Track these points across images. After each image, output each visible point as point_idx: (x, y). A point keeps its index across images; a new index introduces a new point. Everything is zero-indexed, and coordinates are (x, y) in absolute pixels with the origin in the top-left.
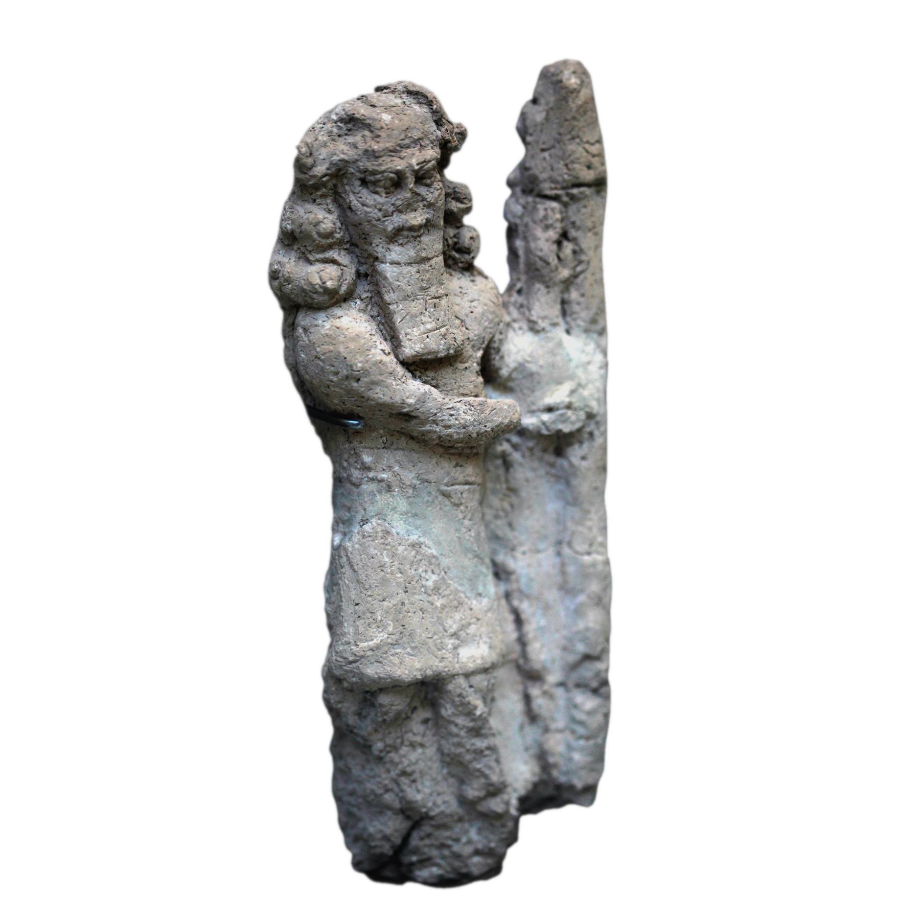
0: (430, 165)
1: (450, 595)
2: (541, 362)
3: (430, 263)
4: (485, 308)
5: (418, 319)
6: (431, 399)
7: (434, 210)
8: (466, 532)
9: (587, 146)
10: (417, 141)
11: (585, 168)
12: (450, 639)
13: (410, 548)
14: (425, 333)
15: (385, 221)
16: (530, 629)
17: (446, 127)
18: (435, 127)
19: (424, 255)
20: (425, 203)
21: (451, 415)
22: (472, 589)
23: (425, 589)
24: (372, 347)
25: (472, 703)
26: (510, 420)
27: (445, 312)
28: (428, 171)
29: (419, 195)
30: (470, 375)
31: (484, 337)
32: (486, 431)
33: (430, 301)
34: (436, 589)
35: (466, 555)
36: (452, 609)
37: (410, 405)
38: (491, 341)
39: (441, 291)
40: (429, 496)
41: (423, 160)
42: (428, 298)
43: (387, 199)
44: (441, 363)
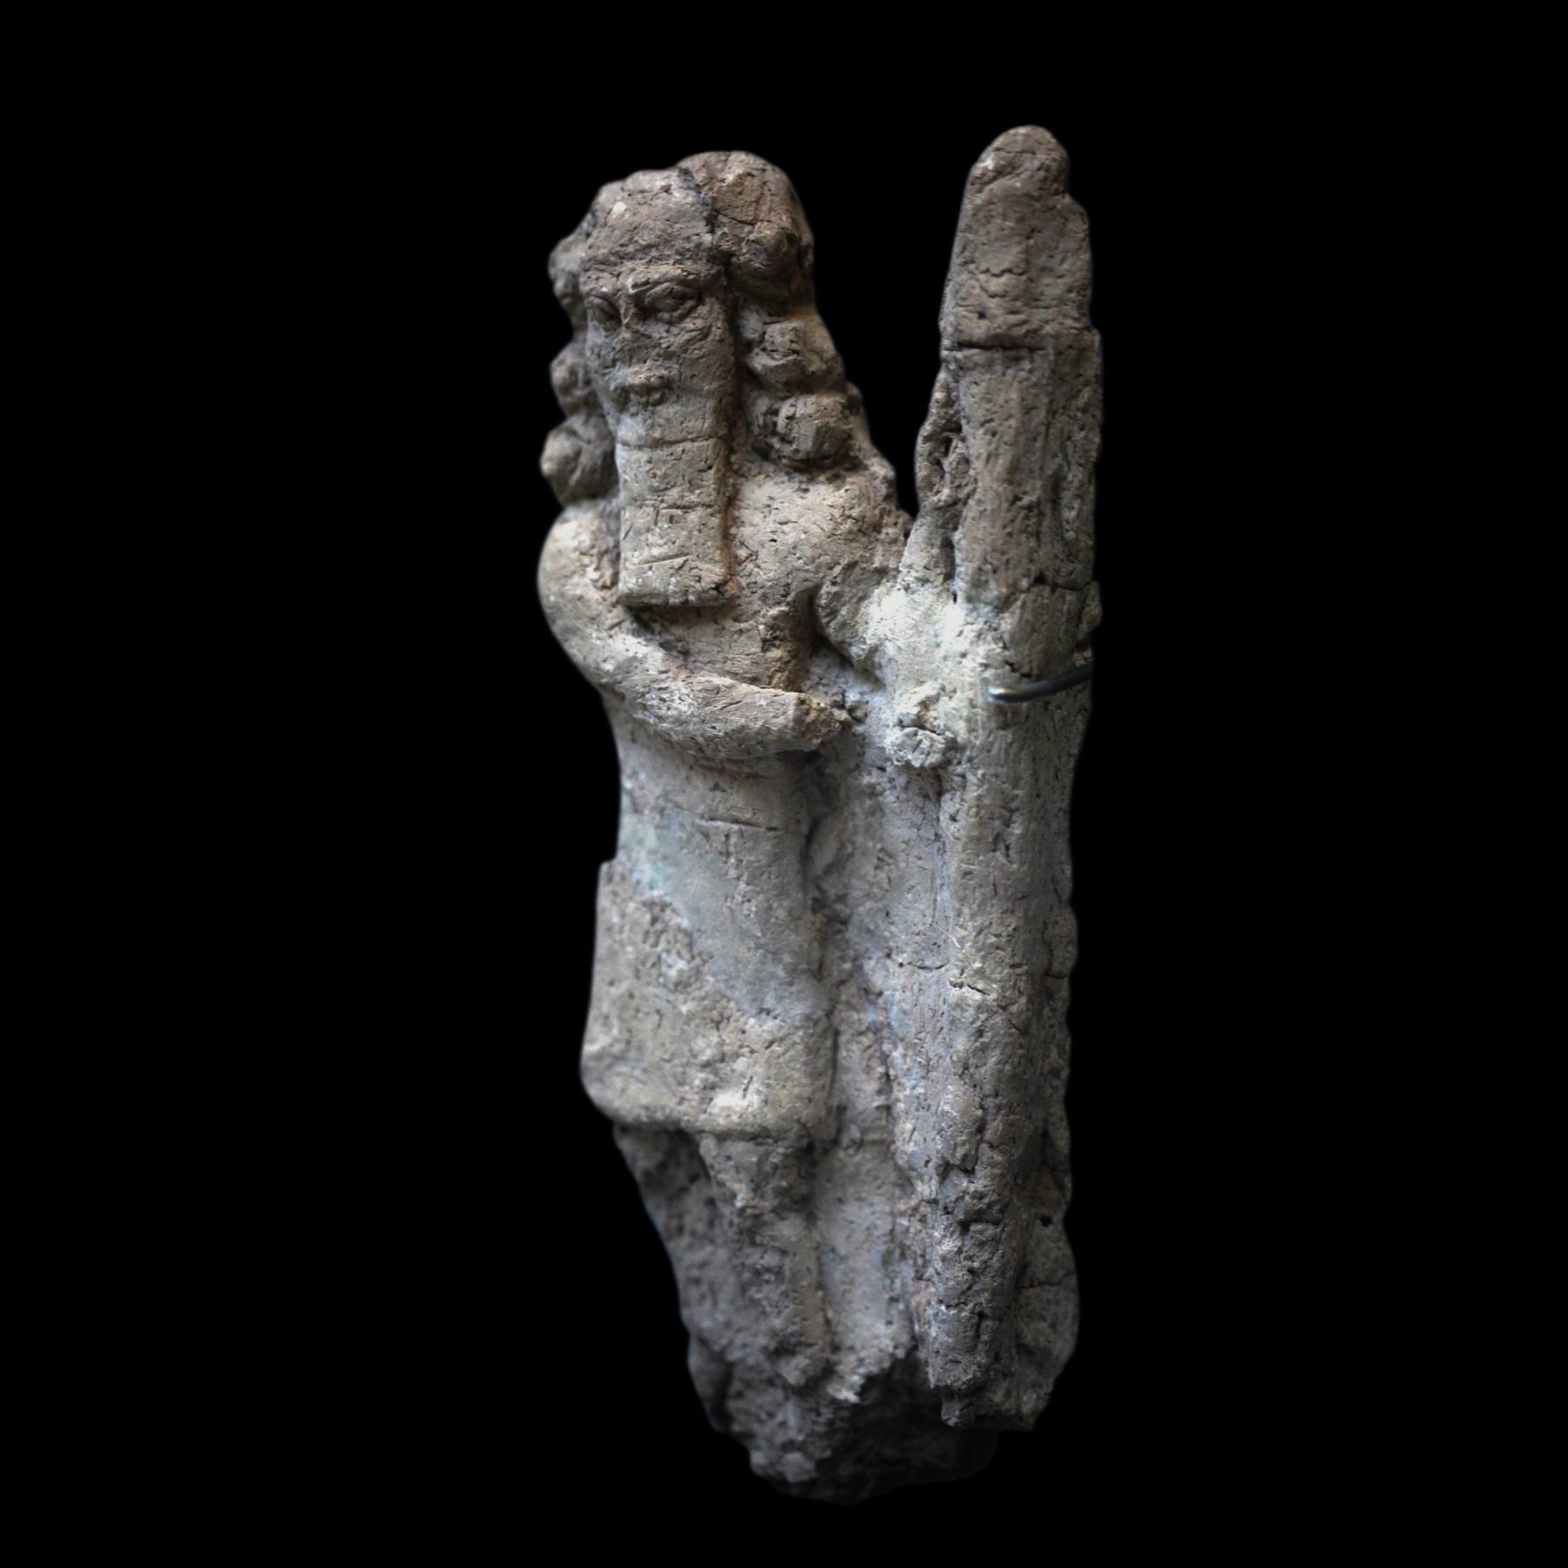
0: (658, 289)
1: (704, 999)
2: (899, 644)
3: (671, 450)
4: (803, 536)
5: (643, 538)
6: (640, 668)
7: (681, 365)
8: (743, 902)
9: (983, 277)
10: (647, 248)
11: (975, 316)
12: (701, 1071)
13: (644, 909)
14: (648, 562)
15: (604, 375)
16: (903, 1095)
17: (726, 230)
18: (701, 227)
19: (657, 434)
20: (657, 350)
21: (664, 701)
22: (754, 1000)
23: (665, 980)
24: (574, 573)
25: (728, 1184)
26: (763, 726)
27: (690, 532)
28: (656, 298)
29: (649, 337)
30: (749, 643)
31: (788, 585)
32: (717, 736)
33: (664, 511)
34: (681, 985)
35: (742, 940)
36: (706, 1024)
37: (607, 673)
38: (811, 595)
39: (692, 497)
40: (682, 831)
41: (643, 280)
42: (664, 505)
43: (608, 340)
44: (699, 615)
